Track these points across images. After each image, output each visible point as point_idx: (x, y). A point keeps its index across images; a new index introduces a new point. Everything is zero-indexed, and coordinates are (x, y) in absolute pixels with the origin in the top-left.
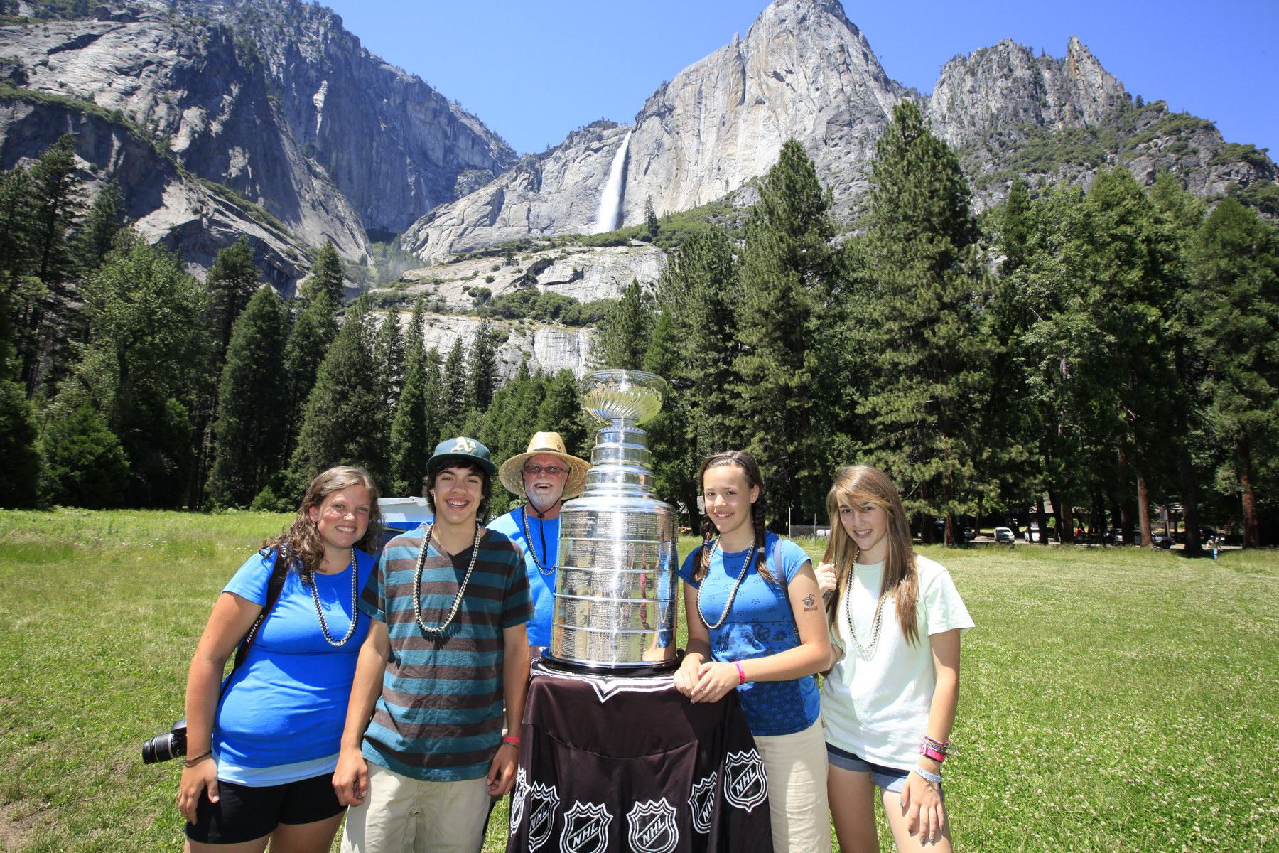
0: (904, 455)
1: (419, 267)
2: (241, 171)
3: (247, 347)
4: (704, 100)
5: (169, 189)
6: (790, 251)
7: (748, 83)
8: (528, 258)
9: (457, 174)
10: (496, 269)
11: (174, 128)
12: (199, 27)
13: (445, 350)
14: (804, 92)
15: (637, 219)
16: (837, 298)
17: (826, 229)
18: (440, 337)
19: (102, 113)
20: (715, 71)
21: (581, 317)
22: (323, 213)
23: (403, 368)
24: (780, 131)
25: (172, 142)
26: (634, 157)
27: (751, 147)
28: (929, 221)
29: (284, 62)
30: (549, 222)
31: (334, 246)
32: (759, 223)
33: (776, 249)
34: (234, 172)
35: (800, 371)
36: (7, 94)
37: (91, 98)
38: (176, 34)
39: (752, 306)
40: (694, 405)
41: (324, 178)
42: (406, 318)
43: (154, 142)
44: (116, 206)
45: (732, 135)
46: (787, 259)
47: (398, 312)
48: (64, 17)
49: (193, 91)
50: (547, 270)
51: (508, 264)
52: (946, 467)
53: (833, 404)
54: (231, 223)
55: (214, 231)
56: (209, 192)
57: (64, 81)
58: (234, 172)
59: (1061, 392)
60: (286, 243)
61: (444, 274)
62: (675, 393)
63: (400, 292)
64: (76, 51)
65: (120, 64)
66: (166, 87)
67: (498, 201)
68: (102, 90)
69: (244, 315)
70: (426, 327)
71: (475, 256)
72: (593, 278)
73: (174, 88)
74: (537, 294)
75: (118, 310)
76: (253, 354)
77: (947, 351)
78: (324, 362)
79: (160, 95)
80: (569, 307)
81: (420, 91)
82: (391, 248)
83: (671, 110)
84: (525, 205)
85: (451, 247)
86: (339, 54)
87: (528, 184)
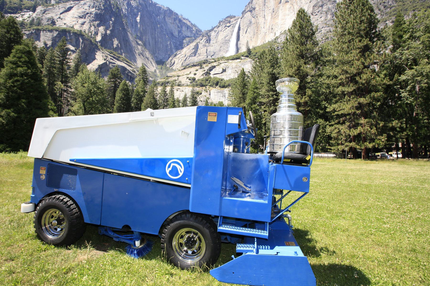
0: (346, 126)
2: (117, 45)
3: (120, 100)
6: (301, 52)
8: (207, 66)
10: (197, 70)
11: (96, 34)
13: (181, 98)
16: (319, 69)
17: (315, 42)
18: (180, 94)
19: (76, 31)
21: (226, 85)
23: (168, 104)
25: (96, 38)
28: (359, 33)
29: (127, 8)
30: (213, 53)
31: (144, 65)
32: (288, 44)
33: (295, 52)
34: (115, 46)
35: (305, 97)
36: (51, 28)
37: (73, 27)
38: (94, 3)
39: (286, 74)
40: (265, 111)
42: (168, 89)
43: (91, 39)
44: (80, 58)
46: (300, 55)
47: (166, 87)
48: (63, 2)
49: (101, 21)
50: (213, 70)
51: (201, 68)
52: (364, 130)
53: (317, 108)
54: (115, 62)
55: (111, 66)
56: (108, 53)
57: (65, 23)
58: (115, 46)
59: (416, 99)
60: (132, 67)
61: (180, 73)
62: (258, 107)
63: (167, 80)
64: (67, 13)
65: (80, 15)
66: (93, 21)
67: (196, 48)
68: (76, 24)
69: (119, 90)
70: (175, 92)
71: (190, 67)
72: (229, 71)
73: (96, 21)
74: (210, 78)
75: (83, 91)
76: (122, 102)
77: (366, 85)
78: (143, 103)
79: (92, 24)
80: (221, 82)
81: (170, 12)
82: (163, 67)
85: (182, 64)
86: (143, 3)
87: (206, 41)
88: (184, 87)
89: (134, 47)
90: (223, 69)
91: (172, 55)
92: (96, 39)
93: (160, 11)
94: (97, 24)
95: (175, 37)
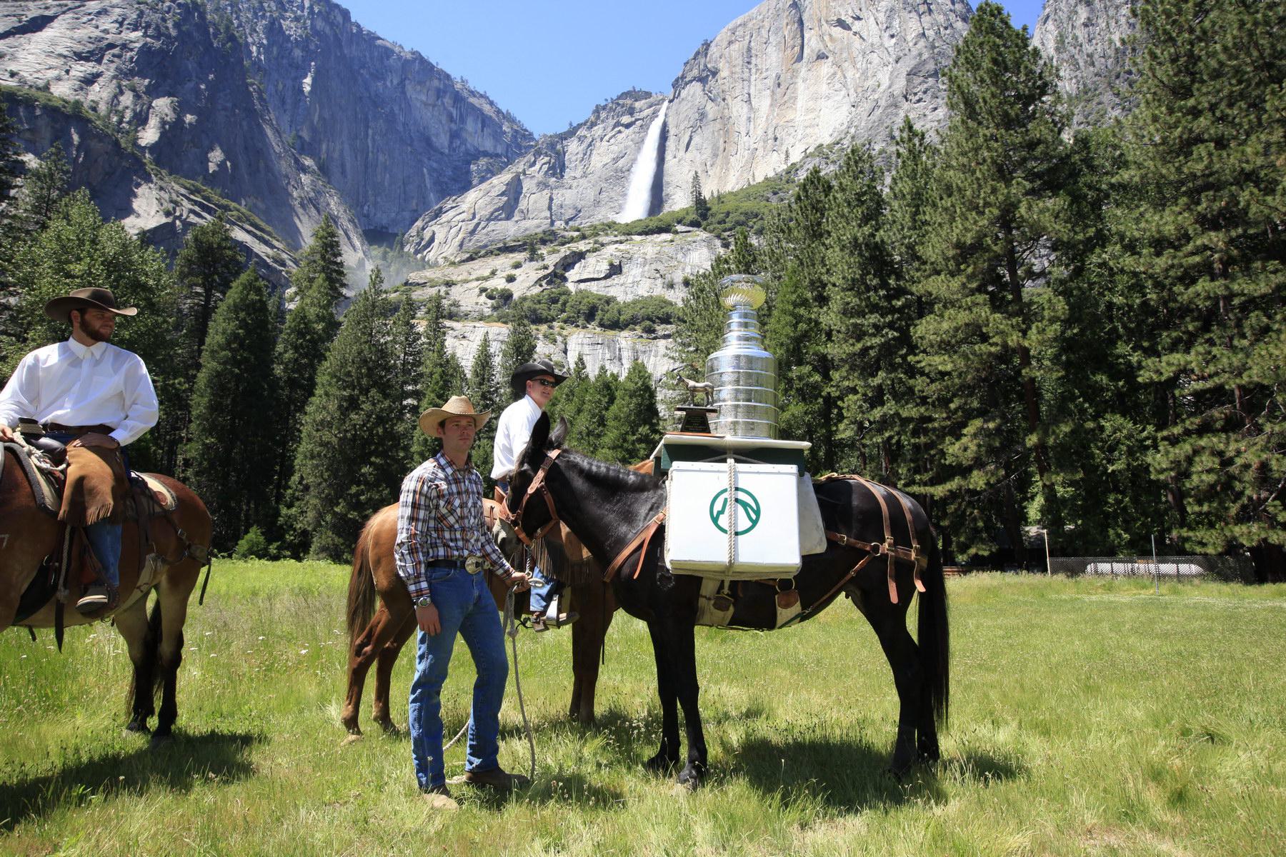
1: (424, 268)
2: (218, 165)
4: (753, 59)
5: (139, 191)
7: (806, 36)
8: (554, 252)
9: (469, 163)
11: (141, 119)
12: (168, 4)
14: (876, 40)
15: (679, 201)
20: (767, 24)
22: (313, 211)
24: (848, 89)
25: (140, 134)
26: (672, 131)
27: (813, 110)
29: (265, 42)
30: (574, 212)
34: (212, 167)
41: (313, 172)
45: (790, 98)
50: (577, 266)
51: (531, 260)
56: (183, 191)
58: (212, 167)
60: (272, 247)
61: (456, 274)
67: (514, 191)
72: (633, 272)
74: (567, 293)
83: (714, 73)
84: (546, 193)
85: (461, 245)
86: (327, 30)
87: (549, 169)
88: (466, 323)
89: (287, 176)
90: (611, 265)
91: (425, 211)
92: (138, 139)
93: (386, 63)
94: (147, 87)
95: (436, 150)
